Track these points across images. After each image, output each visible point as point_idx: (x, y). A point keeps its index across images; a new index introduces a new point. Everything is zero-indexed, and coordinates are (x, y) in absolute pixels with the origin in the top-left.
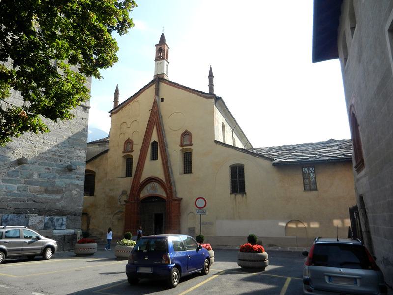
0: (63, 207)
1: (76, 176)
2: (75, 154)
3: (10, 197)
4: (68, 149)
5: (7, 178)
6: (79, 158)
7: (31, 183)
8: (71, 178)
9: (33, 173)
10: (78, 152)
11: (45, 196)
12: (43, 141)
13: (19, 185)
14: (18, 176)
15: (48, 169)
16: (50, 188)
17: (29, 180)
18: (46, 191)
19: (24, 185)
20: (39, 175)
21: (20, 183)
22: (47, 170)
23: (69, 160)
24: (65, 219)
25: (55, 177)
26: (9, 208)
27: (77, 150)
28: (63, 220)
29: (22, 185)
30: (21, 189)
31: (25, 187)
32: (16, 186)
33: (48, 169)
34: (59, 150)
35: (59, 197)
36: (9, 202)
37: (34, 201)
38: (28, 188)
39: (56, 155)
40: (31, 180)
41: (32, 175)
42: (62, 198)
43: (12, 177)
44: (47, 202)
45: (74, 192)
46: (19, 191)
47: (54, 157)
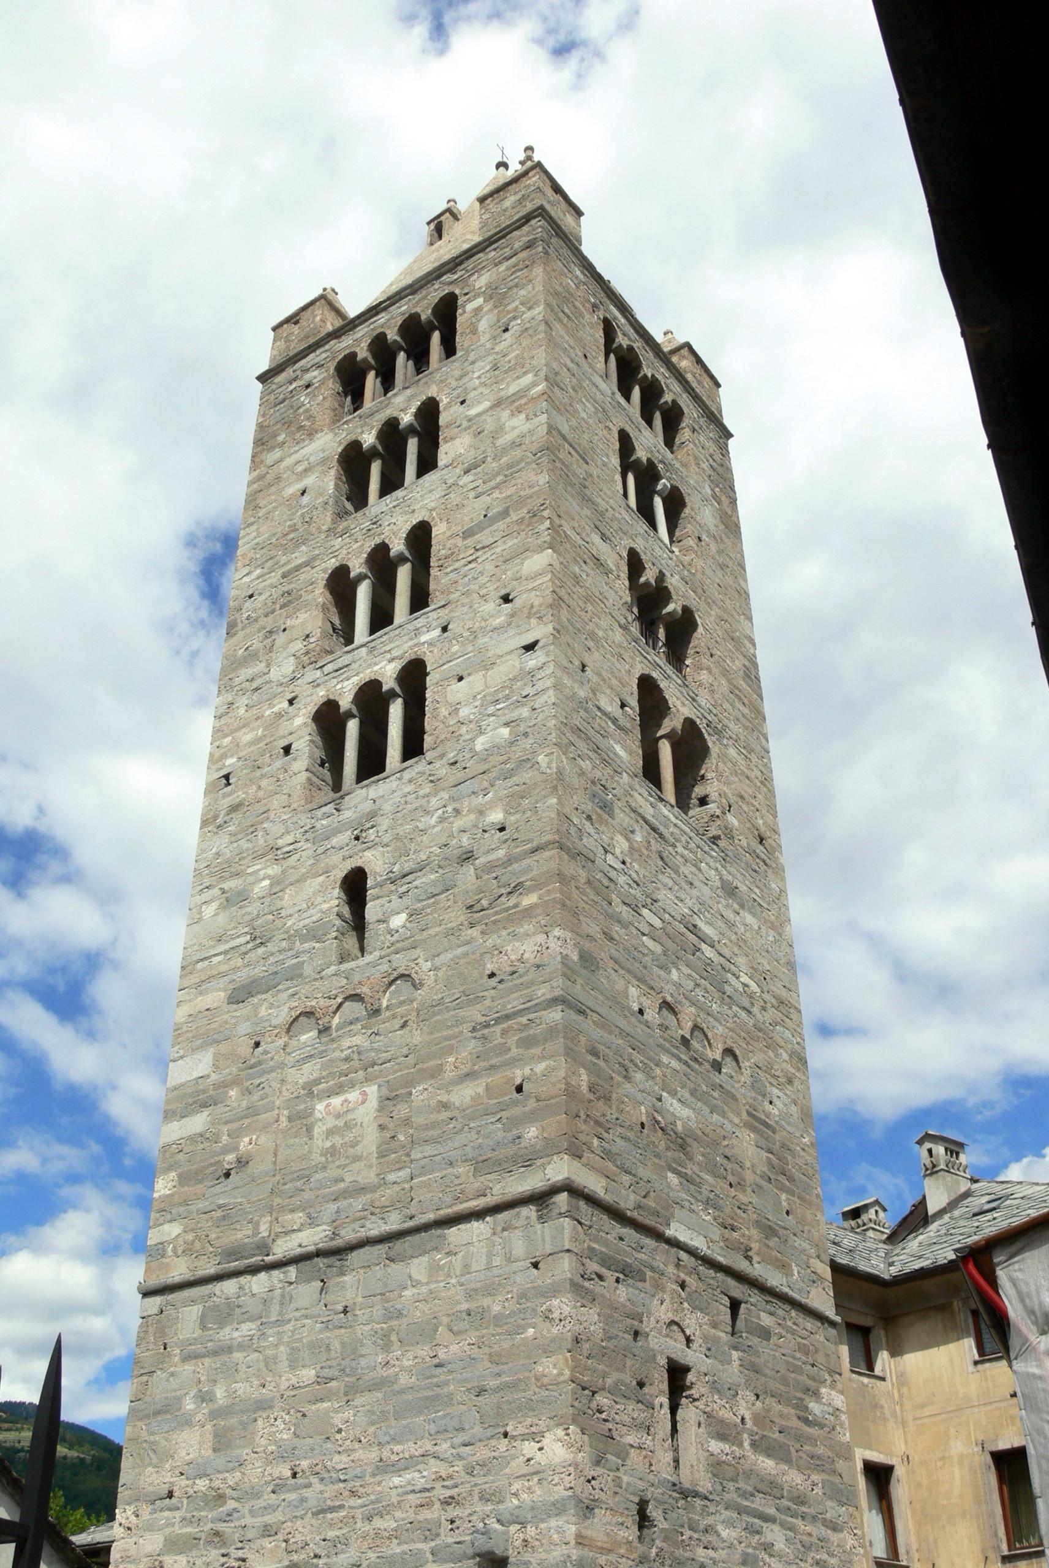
4: (482, 1453)
10: (529, 1448)
12: (373, 1455)
23: (489, 1507)
27: (524, 1438)
47: (426, 1514)
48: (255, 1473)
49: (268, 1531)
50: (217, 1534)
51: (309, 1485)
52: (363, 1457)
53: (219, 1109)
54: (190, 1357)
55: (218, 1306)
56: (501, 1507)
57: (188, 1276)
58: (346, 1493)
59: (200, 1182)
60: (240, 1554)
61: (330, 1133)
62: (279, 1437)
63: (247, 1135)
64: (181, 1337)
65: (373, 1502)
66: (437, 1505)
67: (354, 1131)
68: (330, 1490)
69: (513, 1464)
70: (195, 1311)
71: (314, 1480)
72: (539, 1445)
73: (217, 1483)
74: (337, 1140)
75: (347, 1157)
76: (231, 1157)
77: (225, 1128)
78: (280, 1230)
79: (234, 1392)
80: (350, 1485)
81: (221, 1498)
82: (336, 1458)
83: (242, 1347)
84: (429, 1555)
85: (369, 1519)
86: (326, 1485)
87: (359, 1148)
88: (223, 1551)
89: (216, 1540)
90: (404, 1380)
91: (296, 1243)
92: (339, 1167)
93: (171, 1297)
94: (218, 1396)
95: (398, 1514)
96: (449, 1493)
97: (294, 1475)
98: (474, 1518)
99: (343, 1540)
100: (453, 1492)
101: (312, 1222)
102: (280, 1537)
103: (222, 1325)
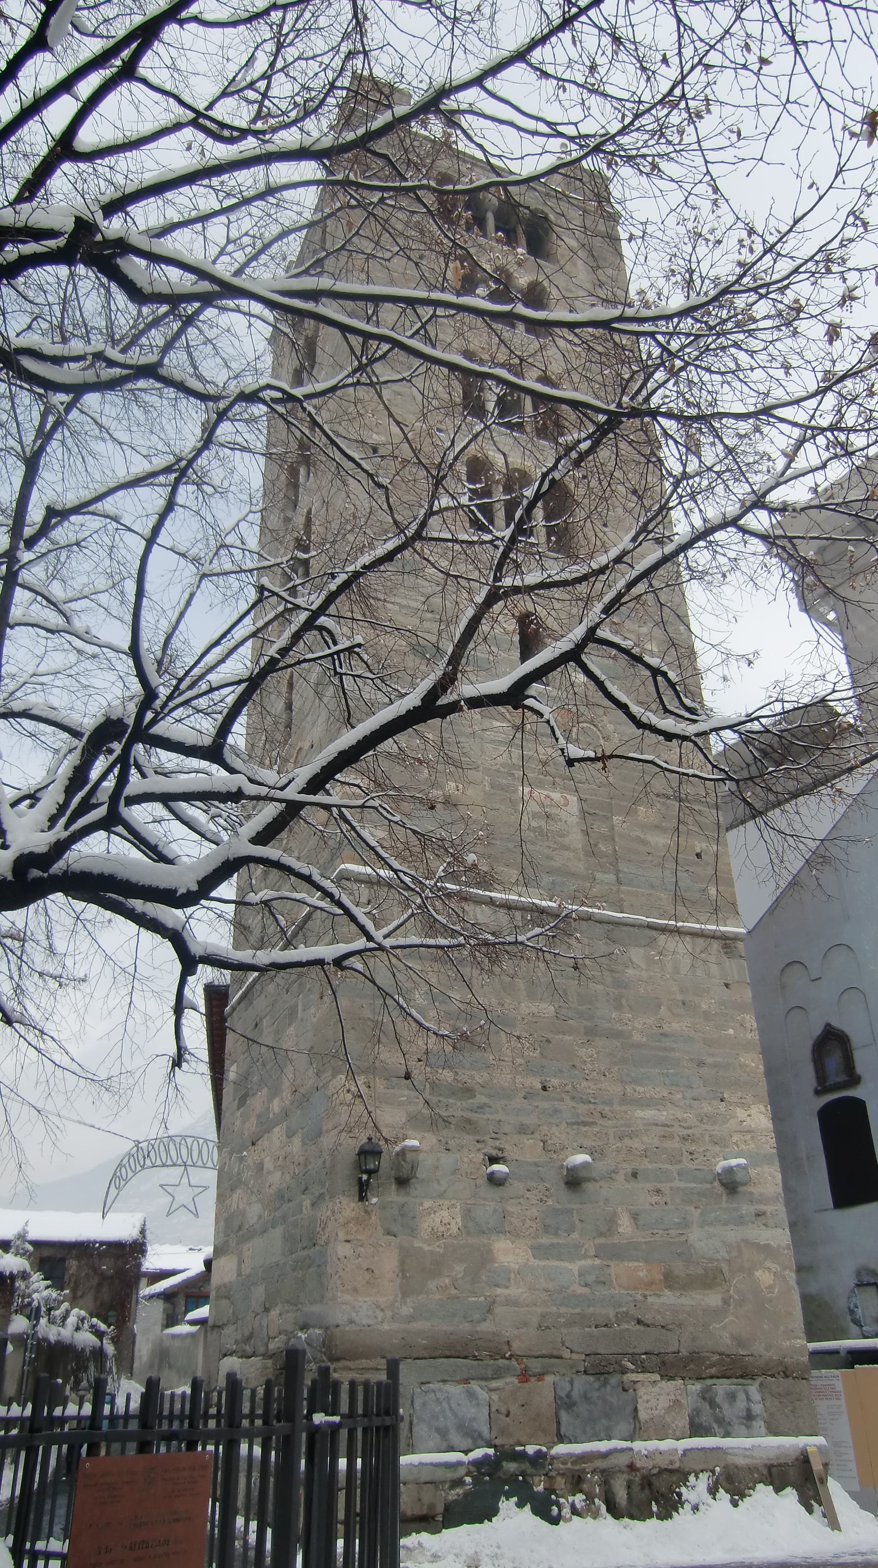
0: (739, 1341)
1: (752, 1209)
2: (732, 1124)
3: (563, 1310)
4: (706, 1108)
5: (545, 1240)
6: (748, 1137)
7: (615, 1253)
8: (740, 1221)
9: (615, 1214)
10: (741, 1113)
11: (669, 1297)
12: (619, 1089)
13: (583, 1263)
14: (571, 1229)
15: (658, 1191)
16: (679, 1268)
18: (670, 1280)
19: (597, 1262)
20: (635, 1217)
21: (585, 1257)
22: (656, 1199)
24: (753, 1389)
25: (685, 1224)
26: (566, 1354)
27: (737, 1105)
28: (748, 1399)
29: (589, 1262)
30: (591, 1279)
32: (575, 1267)
33: (658, 1191)
34: (680, 1114)
35: (713, 1299)
36: (564, 1331)
37: (639, 1322)
38: (612, 1270)
39: (671, 1137)
41: (612, 1221)
42: (726, 1302)
43: (556, 1234)
44: (680, 1326)
45: (764, 1277)
46: (586, 1285)
47: (668, 1144)
48: (503, 1078)
49: (523, 1130)
50: (469, 1121)
56: (726, 1150)
58: (596, 1114)
60: (497, 1143)
66: (677, 1139)
68: (582, 1109)
69: (732, 1121)
72: (748, 1112)
73: (464, 1078)
80: (600, 1107)
81: (468, 1092)
82: (585, 1084)
84: (675, 1175)
85: (621, 1138)
88: (477, 1138)
89: (468, 1127)
90: (637, 1037)
92: (549, 847)
95: (645, 1139)
96: (686, 1132)
97: (544, 1088)
98: (708, 1154)
99: (598, 1149)
100: (690, 1132)
102: (537, 1135)
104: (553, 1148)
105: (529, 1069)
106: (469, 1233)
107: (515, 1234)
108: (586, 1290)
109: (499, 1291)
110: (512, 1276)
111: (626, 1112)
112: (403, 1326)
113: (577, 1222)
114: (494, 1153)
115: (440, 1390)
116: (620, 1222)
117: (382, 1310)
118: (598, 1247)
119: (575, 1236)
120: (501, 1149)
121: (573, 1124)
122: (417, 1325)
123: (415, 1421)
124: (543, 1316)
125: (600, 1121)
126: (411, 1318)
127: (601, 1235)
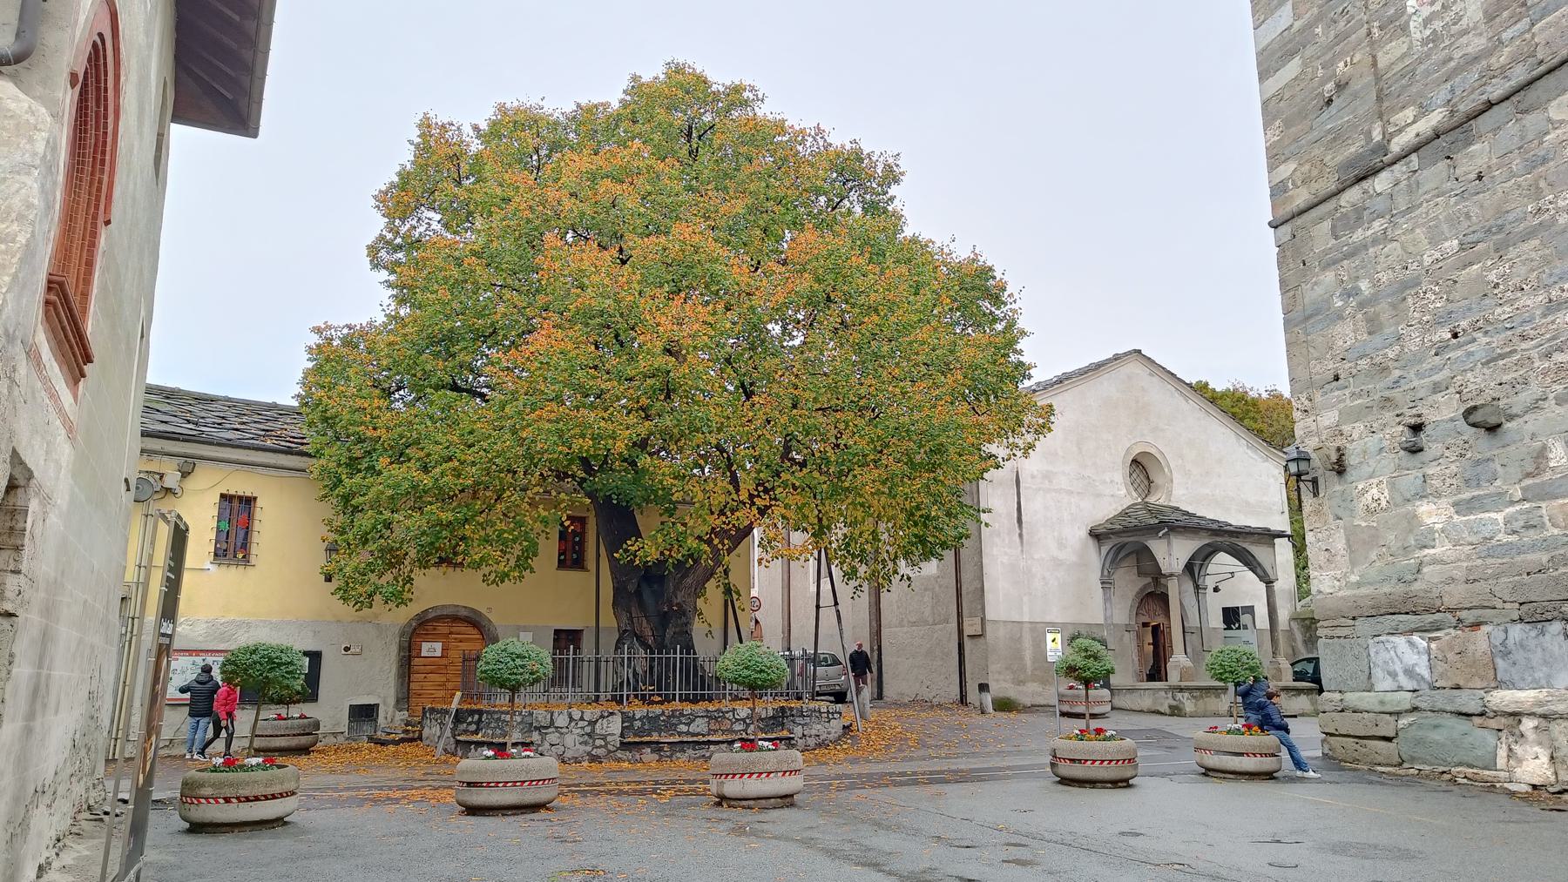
5: (1467, 495)
9: (1544, 448)
12: (1541, 297)
13: (1511, 510)
17: (1537, 480)
21: (1512, 503)
26: (1499, 604)
30: (1517, 525)
31: (1528, 512)
32: (1500, 517)
38: (1544, 511)
40: (1547, 476)
43: (1478, 485)
46: (1514, 532)
49: (1436, 388)
50: (1387, 399)
51: (1474, 340)
52: (1528, 302)
53: (1310, 51)
54: (1329, 265)
55: (1346, 214)
57: (1310, 199)
59: (1305, 118)
60: (1414, 411)
61: (1427, 22)
62: (1432, 307)
63: (1340, 61)
64: (1317, 251)
65: (1549, 340)
67: (1453, 8)
68: (1497, 340)
70: (1327, 225)
71: (1478, 335)
73: (1378, 360)
74: (1438, 25)
75: (1452, 36)
76: (1330, 86)
77: (1318, 64)
78: (1393, 130)
79: (1378, 281)
80: (1519, 330)
81: (1384, 370)
82: (1499, 310)
83: (1375, 242)
85: (1548, 355)
86: (1492, 337)
87: (1464, 22)
88: (1398, 412)
89: (1388, 405)
91: (1412, 134)
93: (1299, 221)
94: (1363, 288)
97: (1455, 336)
99: (1520, 380)
101: (1424, 111)
102: (1452, 390)
103: (1353, 230)
104: (1470, 395)
105: (1439, 322)
106: (1396, 505)
107: (1438, 495)
108: (1512, 538)
109: (1427, 551)
110: (1437, 535)
111: (1553, 322)
112: (1354, 592)
113: (1499, 468)
114: (1412, 421)
115: (1388, 641)
116: (1551, 456)
117: (1339, 580)
118: (1524, 490)
119: (1498, 483)
120: (1419, 416)
121: (1488, 362)
122: (1364, 591)
123: (1372, 665)
124: (1469, 569)
125: (1524, 345)
126: (1359, 585)
127: (1528, 475)
